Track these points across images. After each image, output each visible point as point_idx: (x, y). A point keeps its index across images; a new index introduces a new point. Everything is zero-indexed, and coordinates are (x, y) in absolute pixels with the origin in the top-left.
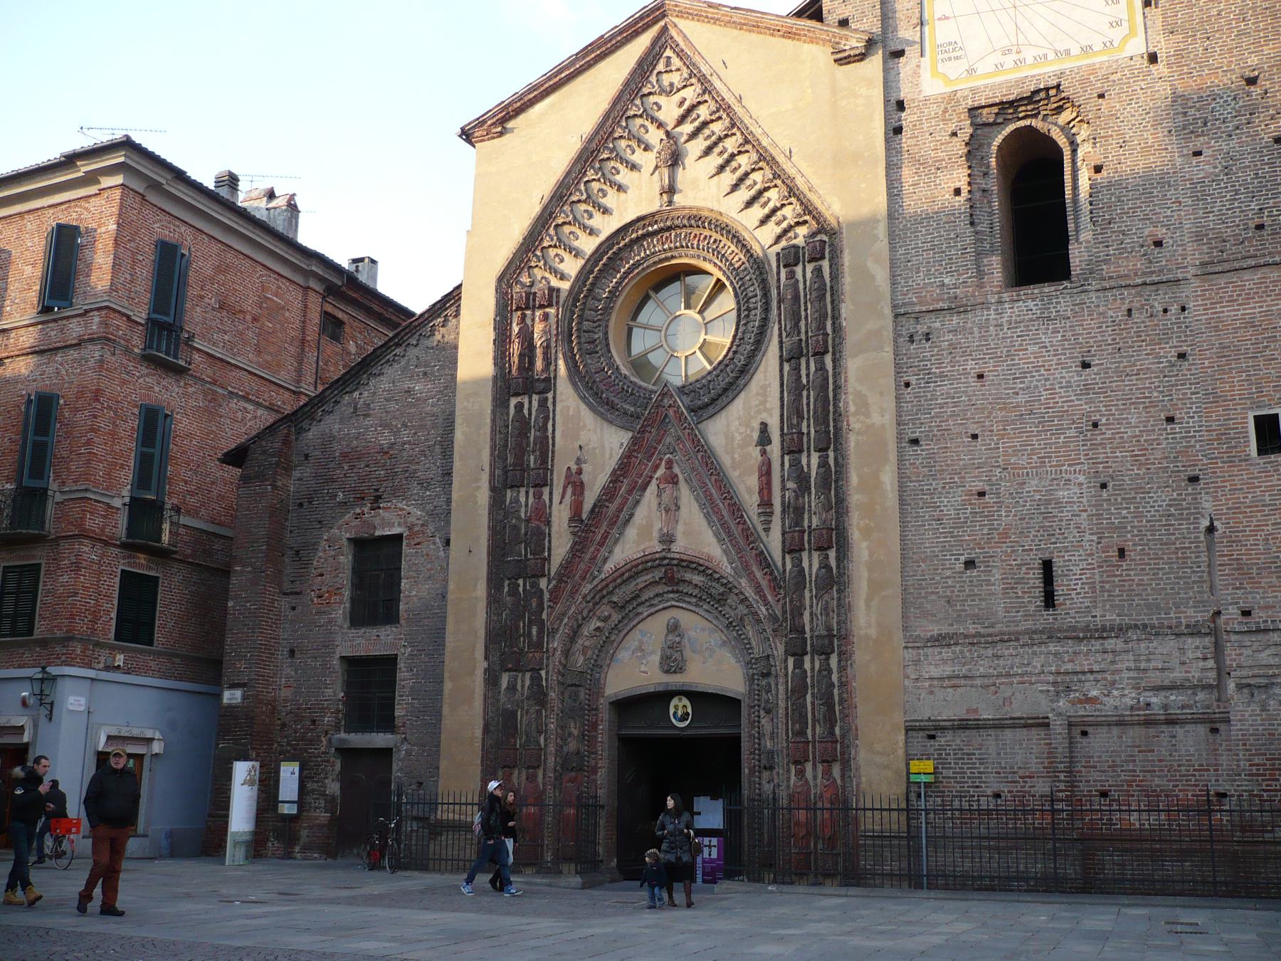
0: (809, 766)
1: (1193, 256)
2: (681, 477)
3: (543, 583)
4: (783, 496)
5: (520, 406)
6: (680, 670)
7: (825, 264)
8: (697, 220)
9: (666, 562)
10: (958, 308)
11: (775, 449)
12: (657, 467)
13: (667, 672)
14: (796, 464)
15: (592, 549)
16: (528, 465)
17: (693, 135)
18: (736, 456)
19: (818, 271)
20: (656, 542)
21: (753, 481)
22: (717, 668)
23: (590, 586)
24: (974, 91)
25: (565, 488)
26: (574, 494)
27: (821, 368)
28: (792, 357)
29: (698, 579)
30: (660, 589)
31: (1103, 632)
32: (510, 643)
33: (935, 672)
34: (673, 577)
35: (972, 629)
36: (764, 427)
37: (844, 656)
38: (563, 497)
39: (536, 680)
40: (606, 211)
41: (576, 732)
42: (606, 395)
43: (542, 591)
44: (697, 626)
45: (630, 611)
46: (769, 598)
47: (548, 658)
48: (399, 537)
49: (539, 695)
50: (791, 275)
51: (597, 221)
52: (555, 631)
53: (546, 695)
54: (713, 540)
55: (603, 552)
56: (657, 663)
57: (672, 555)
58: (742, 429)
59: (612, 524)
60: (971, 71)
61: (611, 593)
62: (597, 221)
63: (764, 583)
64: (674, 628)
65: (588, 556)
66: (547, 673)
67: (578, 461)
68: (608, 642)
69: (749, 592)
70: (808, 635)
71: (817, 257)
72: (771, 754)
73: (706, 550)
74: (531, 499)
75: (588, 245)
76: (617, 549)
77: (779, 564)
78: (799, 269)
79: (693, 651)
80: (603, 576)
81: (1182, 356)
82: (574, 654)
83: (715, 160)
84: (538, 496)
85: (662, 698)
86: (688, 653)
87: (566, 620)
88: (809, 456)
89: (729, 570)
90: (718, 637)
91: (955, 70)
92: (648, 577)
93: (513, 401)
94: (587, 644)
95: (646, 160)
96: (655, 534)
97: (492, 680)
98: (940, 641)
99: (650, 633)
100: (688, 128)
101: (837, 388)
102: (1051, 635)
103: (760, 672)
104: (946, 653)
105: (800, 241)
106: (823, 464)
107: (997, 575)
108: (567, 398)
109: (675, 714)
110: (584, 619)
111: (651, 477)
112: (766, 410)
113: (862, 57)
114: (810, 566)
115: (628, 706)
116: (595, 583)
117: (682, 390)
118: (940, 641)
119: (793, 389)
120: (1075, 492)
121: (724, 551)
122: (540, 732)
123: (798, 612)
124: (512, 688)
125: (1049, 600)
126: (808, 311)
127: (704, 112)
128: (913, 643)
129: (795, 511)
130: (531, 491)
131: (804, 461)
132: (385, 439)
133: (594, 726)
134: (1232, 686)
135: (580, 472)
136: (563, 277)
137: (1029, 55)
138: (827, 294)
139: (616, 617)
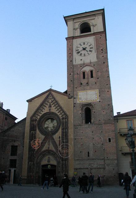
1: (103, 122)
5: (32, 132)
6: (50, 162)
7: (67, 120)
8: (53, 113)
10: (80, 125)
11: (61, 139)
14: (63, 141)
17: (53, 104)
19: (66, 120)
21: (58, 142)
22: (54, 162)
24: (83, 103)
27: (66, 130)
28: (63, 129)
29: (52, 152)
31: (93, 159)
32: (30, 159)
33: (77, 163)
35: (81, 159)
36: (60, 136)
37: (68, 161)
40: (43, 111)
42: (43, 132)
44: (51, 157)
45: (44, 156)
48: (17, 146)
49: (34, 164)
50: (63, 120)
51: (42, 112)
60: (82, 101)
62: (42, 112)
64: (49, 158)
68: (41, 159)
71: (66, 119)
72: (59, 172)
75: (41, 115)
78: (64, 120)
81: (102, 132)
83: (55, 107)
85: (47, 165)
91: (80, 101)
92: (46, 152)
93: (32, 132)
95: (47, 106)
97: (28, 163)
98: (78, 160)
99: (46, 158)
100: (52, 103)
101: (68, 133)
102: (88, 159)
103: (58, 163)
104: (78, 161)
105: (64, 117)
106: (66, 141)
107: (83, 153)
108: (38, 131)
113: (71, 98)
115: (43, 166)
117: (51, 132)
118: (78, 160)
119: (63, 132)
120: (91, 145)
124: (31, 164)
125: (89, 156)
126: (64, 124)
127: (54, 102)
128: (75, 160)
132: (16, 134)
134: (106, 165)
136: (38, 118)
137: (88, 100)
138: (67, 123)
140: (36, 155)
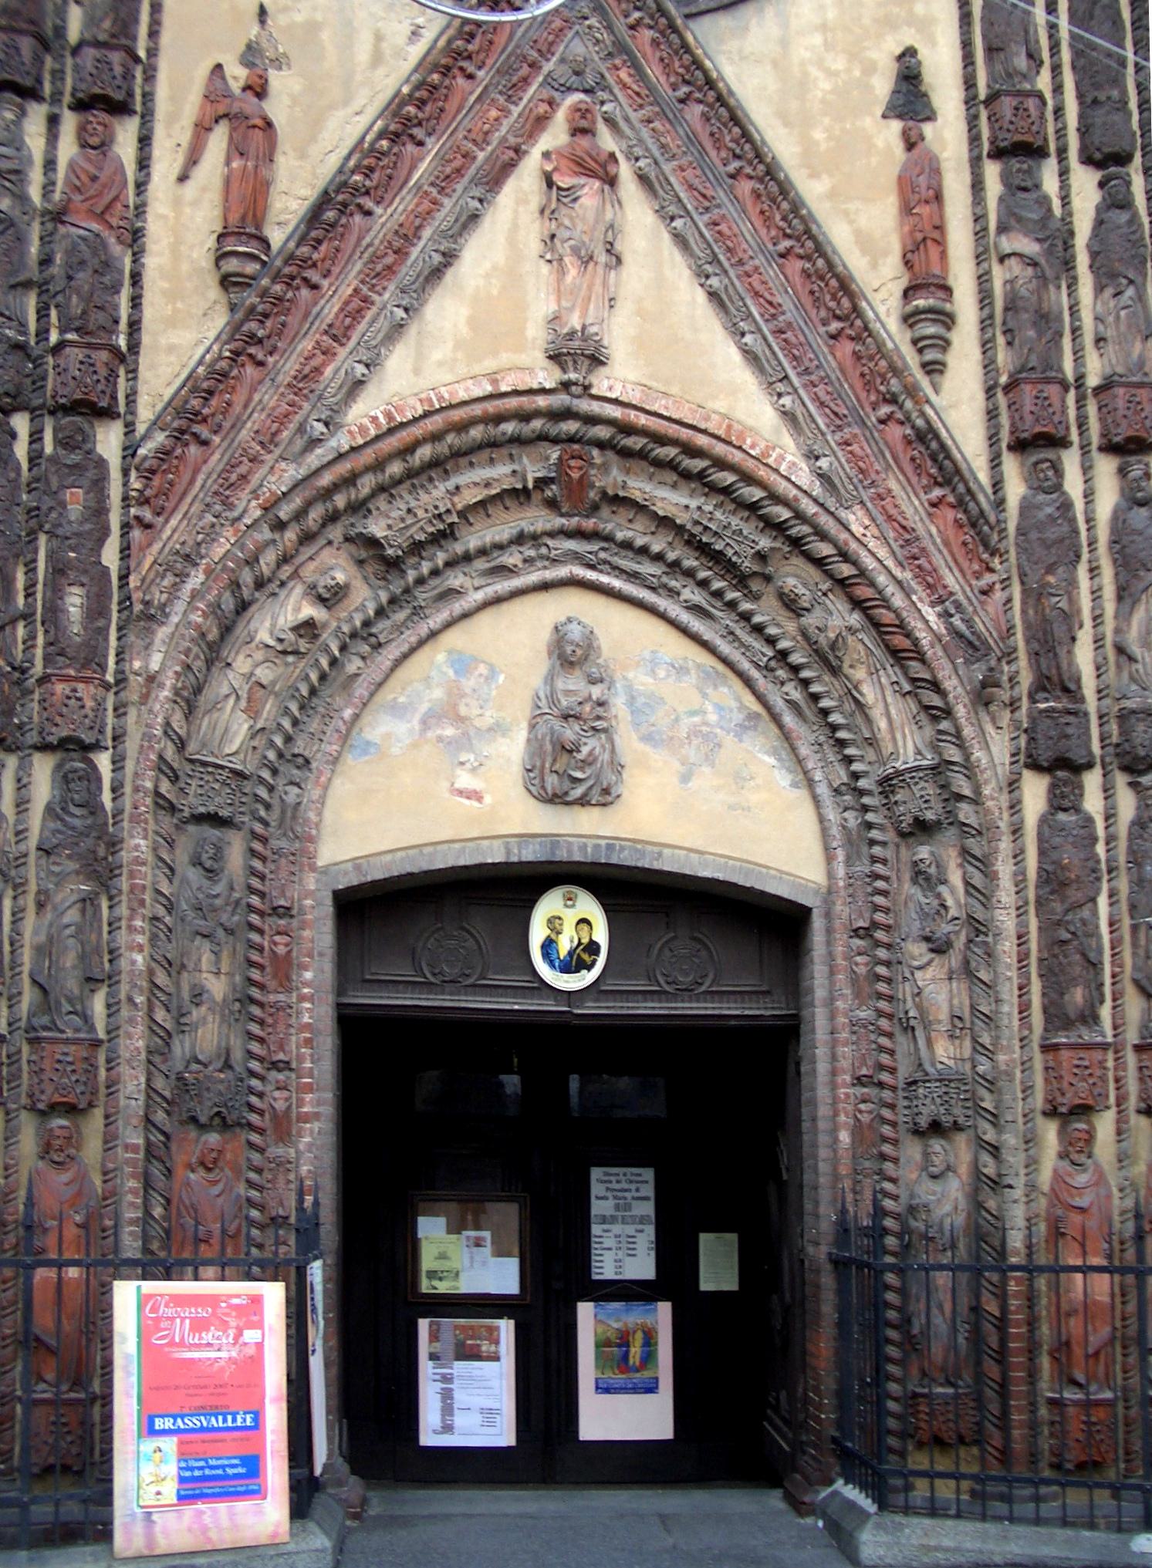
0: (1105, 1125)
2: (625, 171)
3: (109, 441)
4: (983, 281)
6: (604, 796)
9: (571, 427)
11: (948, 133)
12: (540, 122)
13: (556, 799)
14: (1021, 188)
15: (307, 345)
16: (60, 31)
18: (818, 135)
20: (536, 357)
22: (721, 791)
23: (291, 472)
25: (202, 129)
26: (237, 149)
29: (673, 500)
30: (536, 519)
34: (584, 483)
38: (193, 159)
39: (79, 786)
41: (217, 988)
43: (102, 463)
45: (412, 579)
46: (951, 580)
47: (120, 710)
52: (152, 617)
53: (114, 844)
54: (746, 379)
55: (344, 362)
56: (516, 770)
57: (596, 408)
58: (839, 64)
59: (379, 274)
61: (359, 508)
63: (930, 531)
66: (118, 763)
67: (251, 54)
69: (877, 555)
70: (1091, 704)
73: (720, 405)
74: (67, 148)
76: (398, 363)
77: (984, 477)
79: (647, 738)
82: (216, 706)
84: (97, 146)
85: (504, 890)
86: (628, 741)
87: (196, 579)
88: (1064, 173)
89: (804, 476)
90: (731, 696)
92: (499, 473)
94: (264, 674)
96: (536, 334)
99: (496, 655)
103: (899, 818)
109: (548, 946)
110: (260, 584)
111: (519, 152)
112: (912, 21)
114: (1089, 495)
115: (382, 909)
116: (314, 459)
121: (788, 416)
122: (91, 981)
123: (1050, 638)
129: (1026, 325)
130: (69, 122)
131: (1050, 184)
133: (284, 969)
135: (258, 90)
140: (174, 531)
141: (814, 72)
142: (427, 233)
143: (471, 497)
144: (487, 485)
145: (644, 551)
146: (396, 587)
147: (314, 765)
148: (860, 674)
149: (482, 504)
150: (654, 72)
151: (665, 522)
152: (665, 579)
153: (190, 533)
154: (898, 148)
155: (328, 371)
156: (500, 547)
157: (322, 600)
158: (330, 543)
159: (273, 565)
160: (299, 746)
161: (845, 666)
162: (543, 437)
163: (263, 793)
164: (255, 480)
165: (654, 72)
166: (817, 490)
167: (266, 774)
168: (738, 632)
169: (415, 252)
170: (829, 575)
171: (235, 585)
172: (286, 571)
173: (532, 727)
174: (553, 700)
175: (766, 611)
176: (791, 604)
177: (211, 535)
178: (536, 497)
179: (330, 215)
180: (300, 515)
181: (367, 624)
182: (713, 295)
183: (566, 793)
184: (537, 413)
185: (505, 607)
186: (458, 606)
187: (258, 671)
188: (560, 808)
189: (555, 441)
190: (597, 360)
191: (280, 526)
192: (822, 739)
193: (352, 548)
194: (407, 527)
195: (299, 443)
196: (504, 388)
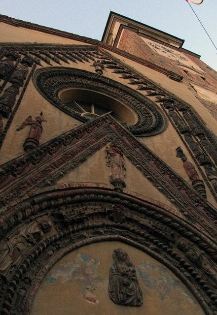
15: (48, 165)
20: (108, 183)
29: (145, 221)
65: (42, 168)
80: (56, 187)
86: (143, 286)
89: (181, 216)
94: (20, 246)
110: (24, 218)
116: (47, 189)
139: (54, 233)
141: (160, 149)
142: (79, 154)
143: (90, 211)
144: (94, 210)
145: (138, 233)
146: (66, 232)
147: (32, 283)
148: (208, 267)
149: (92, 214)
150: (127, 142)
151: (143, 227)
152: (145, 242)
153: (5, 196)
154: (182, 162)
155: (53, 172)
156: (98, 227)
157: (43, 229)
158: (47, 214)
159: (30, 213)
160: (28, 275)
161: (203, 265)
162: (109, 201)
163: (12, 289)
164: (28, 189)
165: (127, 142)
166: (185, 219)
167: (14, 282)
168: (168, 257)
169: (76, 156)
170: (192, 241)
171: (16, 216)
172: (33, 217)
173: (111, 278)
174: (118, 270)
175: (175, 251)
176: (182, 249)
177: (12, 199)
178: (107, 216)
179: (57, 143)
180: (40, 203)
181: (56, 240)
182: (149, 179)
183: (125, 301)
184: (109, 194)
185: (98, 244)
186: (85, 241)
187: (18, 244)
188: (122, 307)
189: (113, 203)
190: (124, 185)
191: (34, 203)
192: (199, 288)
193: (53, 218)
194: (71, 215)
195: (43, 184)
196: (100, 186)
